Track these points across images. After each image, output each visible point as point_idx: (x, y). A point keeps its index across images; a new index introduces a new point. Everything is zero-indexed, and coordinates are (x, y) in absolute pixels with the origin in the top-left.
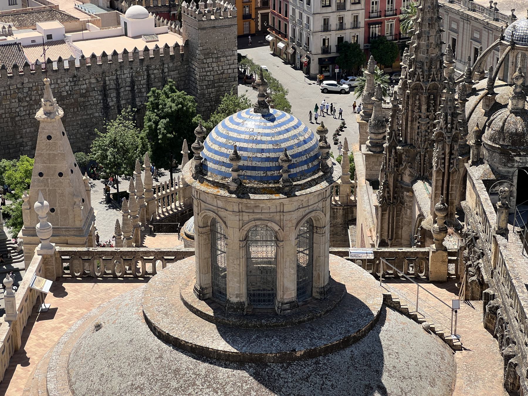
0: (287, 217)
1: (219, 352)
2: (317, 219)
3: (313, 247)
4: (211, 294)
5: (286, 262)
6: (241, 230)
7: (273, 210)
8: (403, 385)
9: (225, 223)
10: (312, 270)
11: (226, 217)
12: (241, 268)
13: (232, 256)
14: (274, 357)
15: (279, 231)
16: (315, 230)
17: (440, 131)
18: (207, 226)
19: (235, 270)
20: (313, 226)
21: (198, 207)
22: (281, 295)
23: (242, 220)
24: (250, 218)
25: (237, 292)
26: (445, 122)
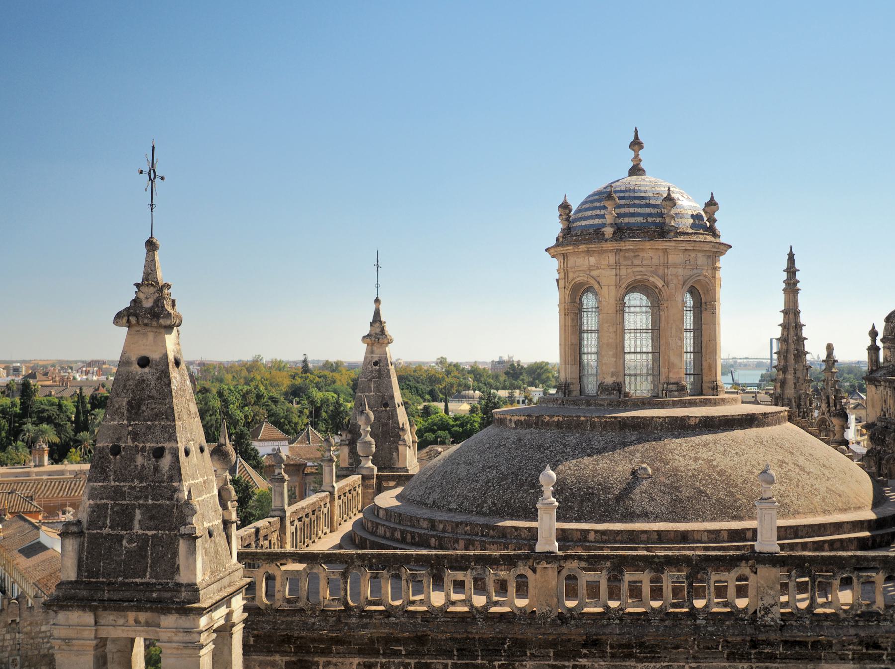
0: (670, 271)
1: (593, 419)
2: (706, 292)
3: (701, 329)
4: (579, 392)
5: (671, 328)
6: (618, 287)
7: (655, 261)
8: (826, 472)
9: (598, 282)
10: (701, 361)
11: (599, 276)
12: (618, 336)
13: (606, 322)
14: (662, 423)
15: (662, 289)
16: (703, 305)
17: (822, 416)
18: (575, 302)
19: (610, 340)
20: (701, 304)
21: (565, 278)
22: (666, 374)
23: (619, 275)
24: (629, 272)
25: (612, 369)
26: (827, 405)
